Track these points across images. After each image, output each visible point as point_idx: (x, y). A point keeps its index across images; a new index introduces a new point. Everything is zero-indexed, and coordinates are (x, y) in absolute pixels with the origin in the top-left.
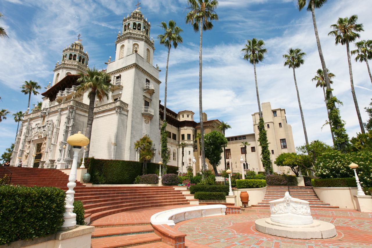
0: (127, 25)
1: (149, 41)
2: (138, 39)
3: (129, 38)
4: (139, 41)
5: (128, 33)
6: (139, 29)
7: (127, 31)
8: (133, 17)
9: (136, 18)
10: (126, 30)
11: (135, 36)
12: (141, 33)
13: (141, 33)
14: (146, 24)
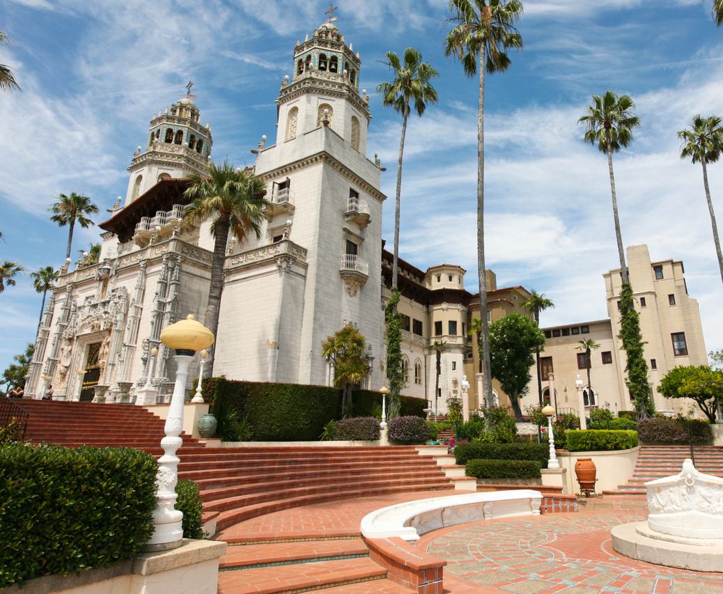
0: (304, 60)
1: (358, 97)
2: (331, 93)
3: (308, 91)
4: (332, 98)
5: (307, 79)
6: (334, 71)
7: (305, 75)
8: (319, 42)
9: (327, 43)
10: (301, 72)
11: (323, 86)
12: (338, 78)
13: (338, 78)
14: (351, 58)
